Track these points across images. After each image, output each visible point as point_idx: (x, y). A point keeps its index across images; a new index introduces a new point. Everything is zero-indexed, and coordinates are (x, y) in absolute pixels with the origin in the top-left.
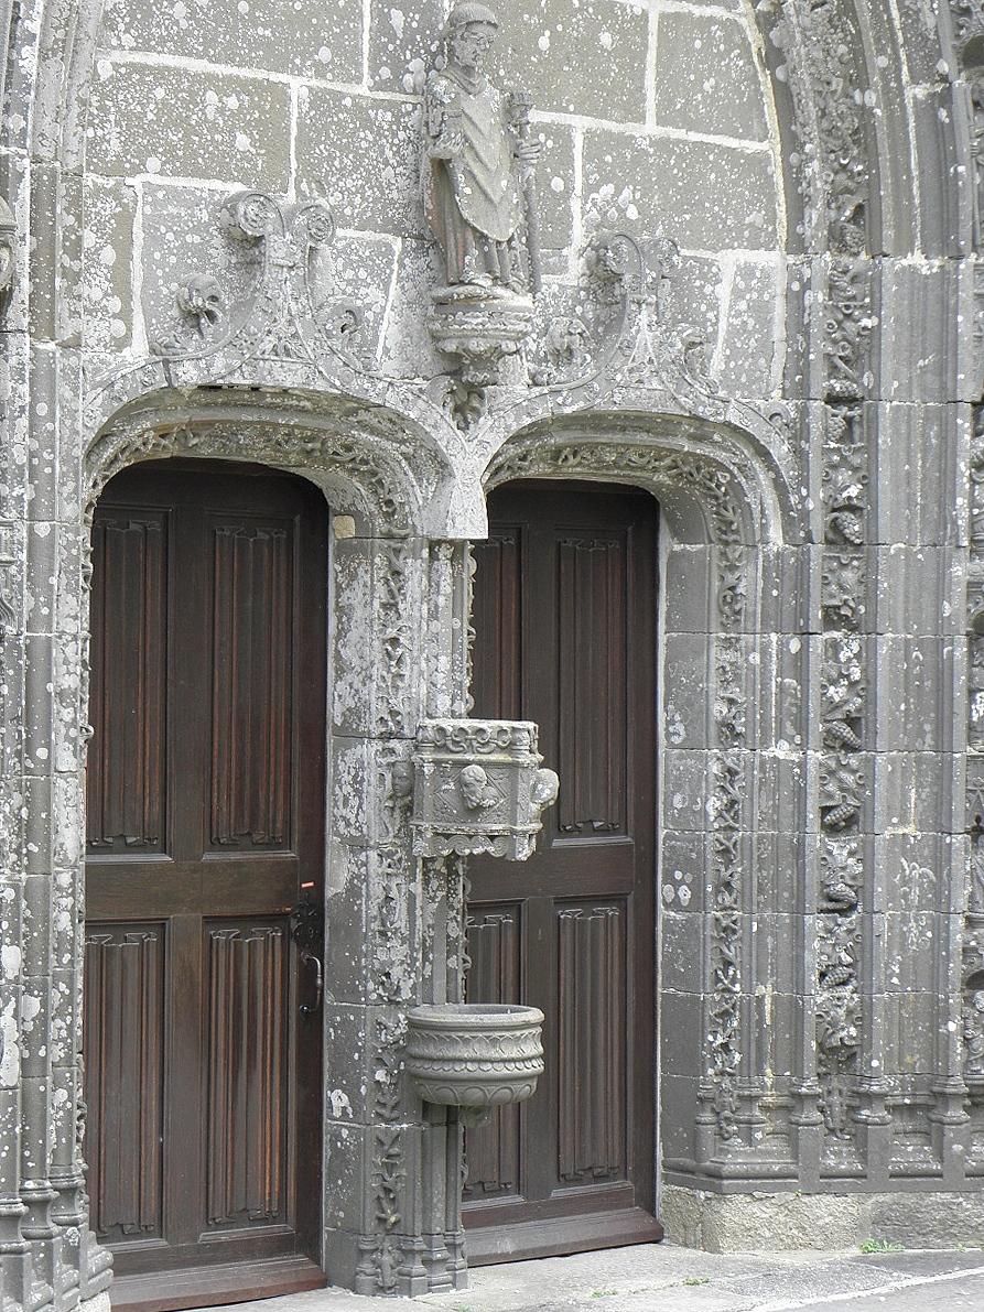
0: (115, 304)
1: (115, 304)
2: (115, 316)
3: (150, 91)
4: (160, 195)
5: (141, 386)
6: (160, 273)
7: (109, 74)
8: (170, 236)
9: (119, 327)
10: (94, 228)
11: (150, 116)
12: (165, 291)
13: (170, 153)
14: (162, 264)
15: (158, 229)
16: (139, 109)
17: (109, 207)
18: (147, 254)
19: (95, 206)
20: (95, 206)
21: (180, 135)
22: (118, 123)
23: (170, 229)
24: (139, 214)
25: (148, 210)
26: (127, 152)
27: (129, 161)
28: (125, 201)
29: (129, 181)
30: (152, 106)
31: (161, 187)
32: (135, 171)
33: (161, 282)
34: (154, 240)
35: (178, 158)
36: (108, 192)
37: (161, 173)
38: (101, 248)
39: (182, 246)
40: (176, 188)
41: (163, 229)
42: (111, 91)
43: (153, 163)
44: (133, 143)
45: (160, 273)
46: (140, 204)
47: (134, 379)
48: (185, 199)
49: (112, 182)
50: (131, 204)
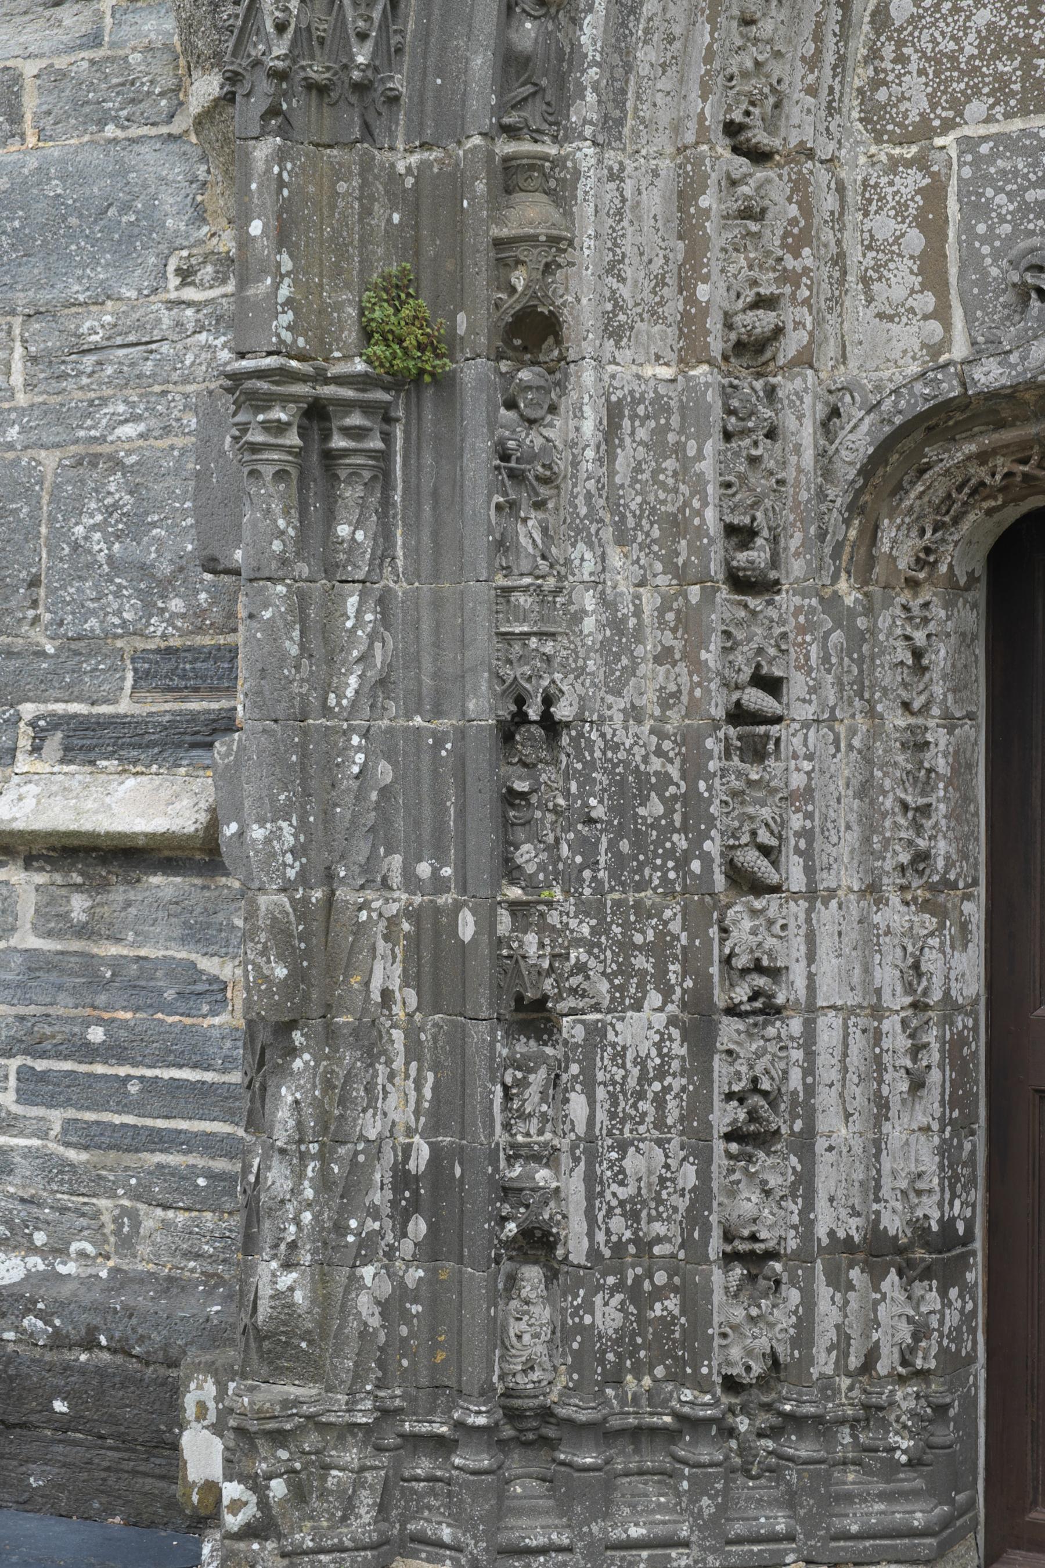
0: (928, 301)
1: (928, 301)
2: (926, 317)
3: (968, 18)
4: (984, 149)
5: (920, 400)
6: (986, 250)
7: (907, 15)
8: (1001, 199)
9: (935, 327)
10: (892, 213)
11: (970, 50)
12: (995, 272)
13: (1001, 86)
14: (988, 238)
15: (983, 194)
16: (952, 45)
17: (912, 180)
18: (966, 228)
19: (891, 184)
20: (891, 184)
21: (1016, 63)
22: (922, 72)
23: (1000, 190)
24: (954, 181)
25: (967, 172)
26: (933, 106)
27: (939, 117)
28: (935, 168)
29: (939, 141)
30: (972, 37)
31: (984, 139)
32: (948, 126)
33: (988, 261)
34: (976, 208)
35: (1013, 94)
36: (909, 164)
37: (989, 119)
38: (903, 235)
39: (1019, 209)
40: (1009, 136)
41: (990, 192)
42: (911, 34)
43: (976, 108)
44: (944, 92)
45: (986, 250)
46: (955, 167)
47: (912, 394)
48: (1025, 146)
49: (914, 149)
50: (944, 171)
